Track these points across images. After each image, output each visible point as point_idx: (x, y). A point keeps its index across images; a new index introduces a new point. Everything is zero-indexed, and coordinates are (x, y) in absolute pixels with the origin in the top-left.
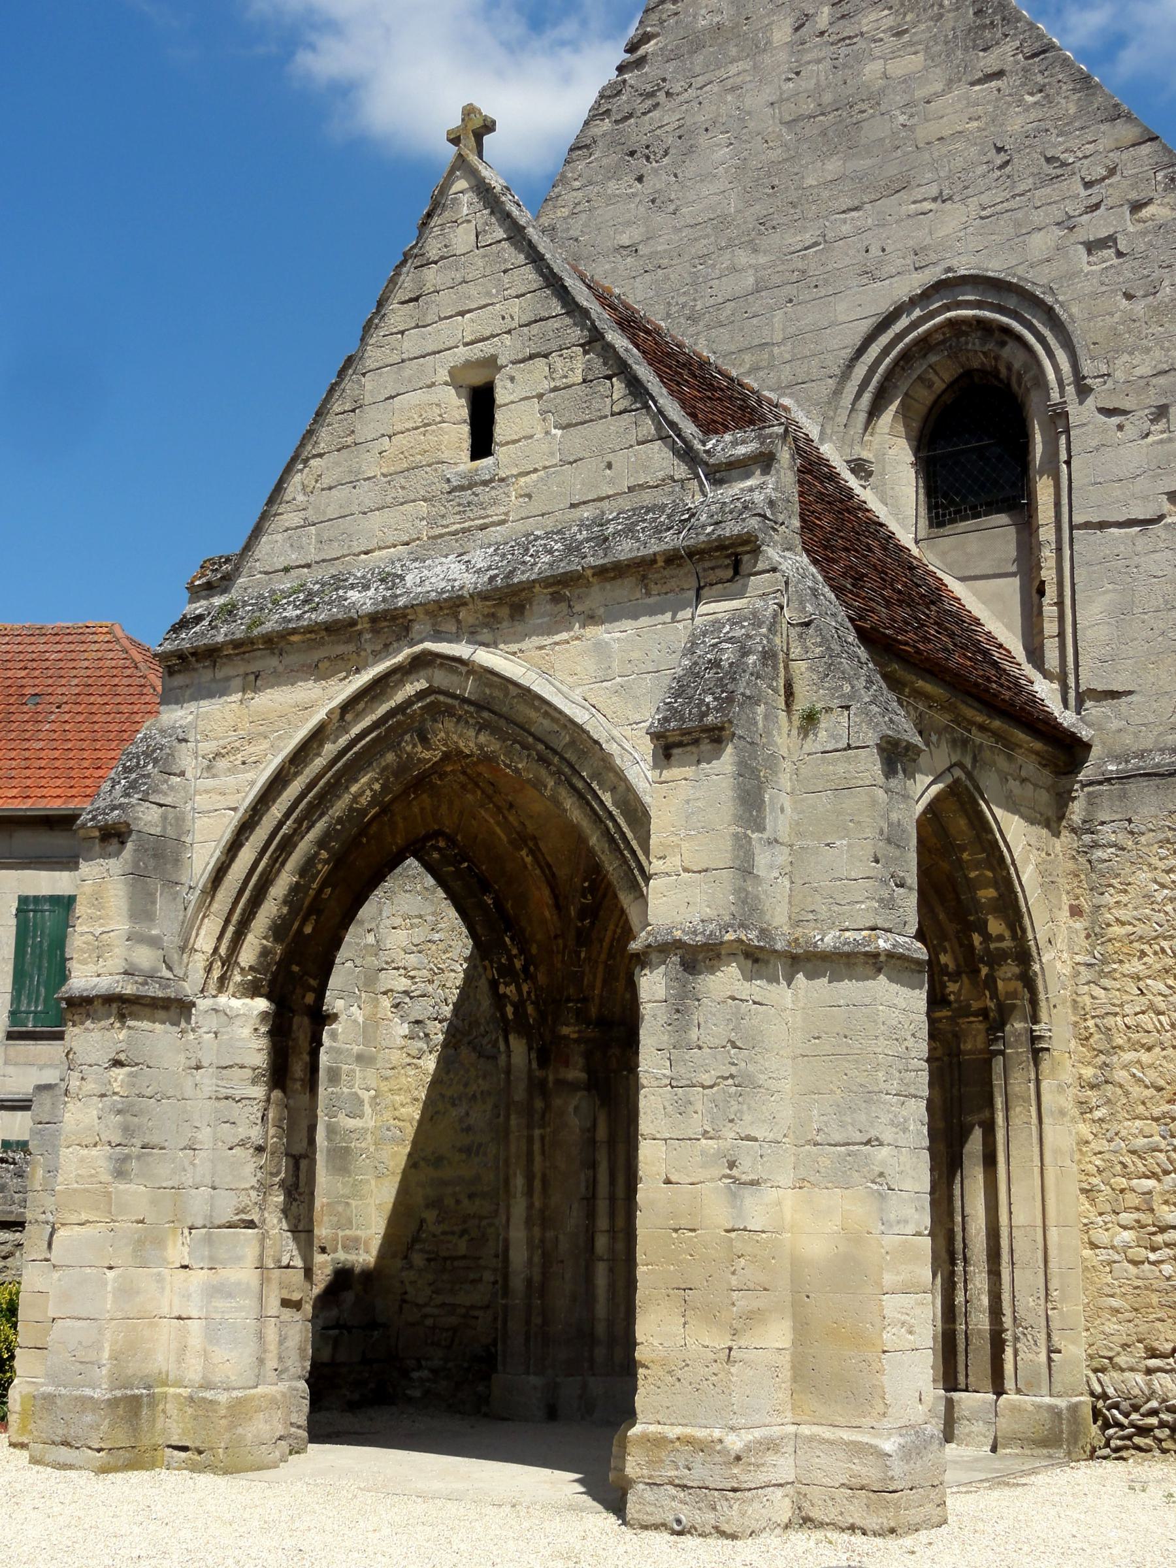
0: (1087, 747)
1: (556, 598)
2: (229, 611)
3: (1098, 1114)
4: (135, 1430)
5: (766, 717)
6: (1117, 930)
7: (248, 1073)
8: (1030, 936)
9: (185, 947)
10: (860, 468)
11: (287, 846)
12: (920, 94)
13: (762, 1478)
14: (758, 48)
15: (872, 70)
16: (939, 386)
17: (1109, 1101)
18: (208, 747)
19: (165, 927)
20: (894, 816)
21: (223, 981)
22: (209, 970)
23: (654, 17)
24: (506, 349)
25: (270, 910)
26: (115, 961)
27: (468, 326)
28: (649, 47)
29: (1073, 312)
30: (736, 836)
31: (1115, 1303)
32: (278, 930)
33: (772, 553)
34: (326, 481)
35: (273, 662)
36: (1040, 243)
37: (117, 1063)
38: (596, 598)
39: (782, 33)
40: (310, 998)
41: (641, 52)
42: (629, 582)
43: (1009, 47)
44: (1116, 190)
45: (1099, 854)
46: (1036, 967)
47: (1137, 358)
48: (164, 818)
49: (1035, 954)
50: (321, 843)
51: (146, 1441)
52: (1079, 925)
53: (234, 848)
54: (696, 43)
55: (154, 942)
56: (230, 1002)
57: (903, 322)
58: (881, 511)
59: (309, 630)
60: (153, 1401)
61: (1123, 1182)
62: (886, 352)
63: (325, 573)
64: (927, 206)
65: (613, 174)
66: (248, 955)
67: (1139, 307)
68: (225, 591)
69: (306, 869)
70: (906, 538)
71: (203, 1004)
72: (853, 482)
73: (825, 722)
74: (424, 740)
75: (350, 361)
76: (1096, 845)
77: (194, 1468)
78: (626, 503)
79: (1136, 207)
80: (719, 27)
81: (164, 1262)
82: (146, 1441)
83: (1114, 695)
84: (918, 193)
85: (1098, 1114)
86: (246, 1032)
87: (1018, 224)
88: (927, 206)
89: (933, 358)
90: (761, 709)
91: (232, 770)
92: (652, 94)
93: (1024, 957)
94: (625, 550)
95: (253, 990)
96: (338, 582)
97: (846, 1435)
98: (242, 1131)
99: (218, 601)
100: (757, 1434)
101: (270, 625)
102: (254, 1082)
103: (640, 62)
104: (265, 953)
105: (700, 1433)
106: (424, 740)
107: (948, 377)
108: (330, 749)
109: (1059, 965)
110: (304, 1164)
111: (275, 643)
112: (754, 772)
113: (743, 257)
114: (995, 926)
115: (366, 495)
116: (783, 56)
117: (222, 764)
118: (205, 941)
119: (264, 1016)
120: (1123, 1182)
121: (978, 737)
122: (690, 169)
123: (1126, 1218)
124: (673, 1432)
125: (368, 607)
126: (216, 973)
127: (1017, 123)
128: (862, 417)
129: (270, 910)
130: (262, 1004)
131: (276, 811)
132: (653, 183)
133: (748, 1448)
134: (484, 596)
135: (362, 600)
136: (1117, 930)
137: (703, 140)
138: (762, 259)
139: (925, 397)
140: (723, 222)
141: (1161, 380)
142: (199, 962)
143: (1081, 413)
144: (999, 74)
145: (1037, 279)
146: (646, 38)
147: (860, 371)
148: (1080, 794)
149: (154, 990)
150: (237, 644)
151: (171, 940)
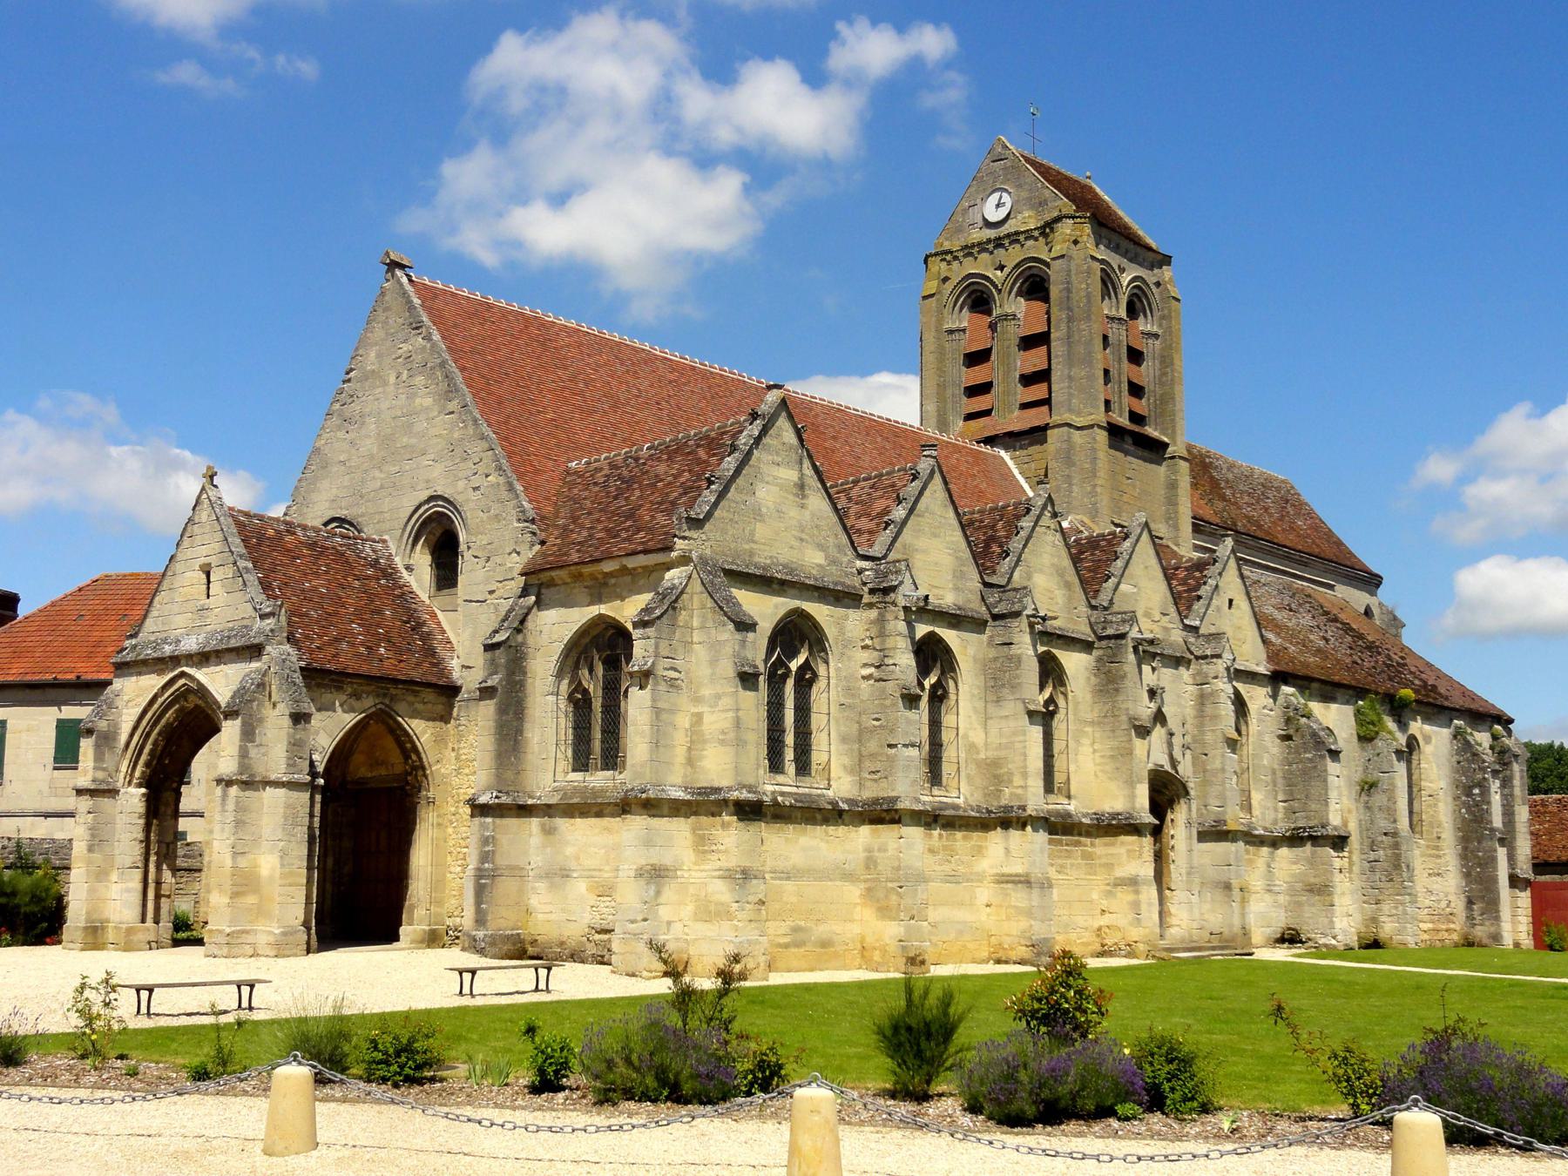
0: (461, 687)
1: (217, 657)
2: (134, 647)
3: (455, 824)
4: (96, 938)
5: (258, 705)
6: (464, 757)
7: (137, 815)
8: (424, 760)
9: (117, 770)
10: (409, 568)
11: (148, 735)
12: (431, 416)
13: (240, 941)
14: (385, 383)
15: (418, 401)
16: (438, 534)
17: (457, 821)
18: (126, 698)
19: (109, 763)
20: (298, 737)
21: (130, 783)
22: (125, 778)
23: (354, 362)
24: (214, 560)
25: (144, 757)
26: (89, 777)
27: (204, 550)
28: (352, 374)
29: (468, 515)
30: (240, 746)
31: (454, 893)
32: (147, 765)
33: (268, 648)
34: (165, 601)
35: (145, 669)
36: (461, 484)
37: (89, 812)
38: (227, 656)
39: (392, 379)
40: (175, 785)
41: (349, 376)
42: (234, 653)
43: (455, 402)
44: (482, 469)
45: (460, 728)
46: (428, 772)
47: (484, 537)
48: (109, 725)
49: (427, 766)
50: (159, 734)
51: (100, 941)
52: (453, 754)
53: (132, 735)
54: (365, 377)
55: (104, 769)
56: (132, 790)
57: (421, 511)
58: (415, 587)
59: (153, 659)
60: (103, 928)
61: (459, 849)
62: (417, 520)
63: (163, 635)
64: (431, 463)
65: (339, 428)
66: (137, 774)
67: (485, 516)
68: (136, 637)
69: (155, 743)
70: (424, 596)
71: (122, 791)
72: (405, 574)
73: (278, 706)
74: (186, 701)
75: (172, 557)
76: (459, 725)
77: (116, 950)
78: (240, 623)
79: (487, 476)
80: (374, 371)
81: (109, 881)
82: (100, 941)
83: (470, 668)
84: (428, 457)
85: (455, 824)
86: (137, 800)
87: (455, 476)
88: (431, 463)
89: (434, 525)
90: (255, 703)
91: (133, 707)
92: (352, 396)
93: (424, 768)
94: (233, 643)
95: (140, 785)
96: (165, 641)
97: (268, 929)
98: (135, 836)
99: (134, 641)
100: (238, 928)
101: (142, 657)
102: (139, 818)
103: (349, 380)
104: (143, 772)
105: (220, 928)
106: (186, 701)
107: (440, 531)
108: (160, 700)
109: (443, 770)
110: (171, 846)
111: (145, 662)
112: (251, 725)
113: (377, 474)
114: (414, 757)
115: (175, 608)
116: (392, 388)
117: (130, 704)
118: (124, 769)
119: (143, 795)
120: (459, 849)
121: (393, 691)
122: (363, 432)
123: (460, 862)
124: (214, 928)
125: (168, 654)
126: (127, 780)
127: (456, 435)
128: (409, 547)
129: (144, 757)
130: (143, 790)
131: (144, 722)
132: (351, 436)
133: (233, 932)
134: (199, 654)
135: (168, 650)
136: (464, 757)
137: (367, 420)
138: (382, 476)
139: (434, 539)
140: (372, 457)
141: (489, 547)
142: (122, 775)
143: (467, 555)
144: (452, 413)
145: (459, 499)
146: (352, 370)
147: (409, 528)
148: (457, 705)
149: (104, 787)
150: (134, 662)
151: (112, 768)
